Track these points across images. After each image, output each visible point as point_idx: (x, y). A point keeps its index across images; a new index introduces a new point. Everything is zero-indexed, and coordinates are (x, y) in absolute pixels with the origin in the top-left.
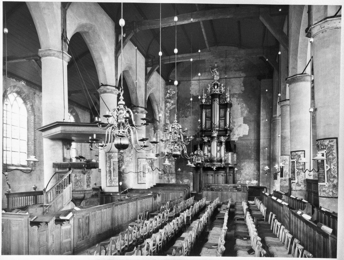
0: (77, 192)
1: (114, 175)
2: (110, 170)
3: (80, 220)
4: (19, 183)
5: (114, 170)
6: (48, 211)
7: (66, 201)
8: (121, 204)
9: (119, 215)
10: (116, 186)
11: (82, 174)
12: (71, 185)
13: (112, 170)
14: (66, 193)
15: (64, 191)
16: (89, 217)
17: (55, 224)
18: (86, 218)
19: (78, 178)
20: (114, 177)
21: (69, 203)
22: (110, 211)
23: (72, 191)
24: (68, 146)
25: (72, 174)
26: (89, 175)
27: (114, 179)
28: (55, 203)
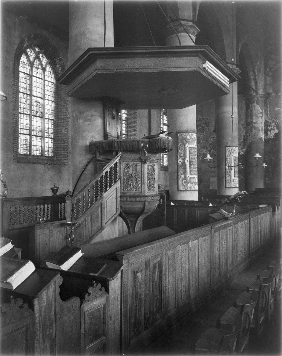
0: (129, 199)
1: (190, 172)
2: (185, 163)
3: (139, 274)
4: (42, 184)
5: (191, 162)
6: (75, 235)
7: (109, 216)
8: (225, 227)
9: (222, 252)
10: (195, 191)
11: (140, 163)
12: (118, 184)
13: (187, 163)
14: (109, 201)
15: (104, 195)
16: (160, 265)
17: (59, 299)
18: (154, 267)
19: (131, 171)
20: (190, 175)
21: (115, 219)
22: (206, 245)
23: (121, 197)
24: (114, 113)
25: (119, 163)
26: (153, 166)
27: (190, 178)
28: (88, 220)
